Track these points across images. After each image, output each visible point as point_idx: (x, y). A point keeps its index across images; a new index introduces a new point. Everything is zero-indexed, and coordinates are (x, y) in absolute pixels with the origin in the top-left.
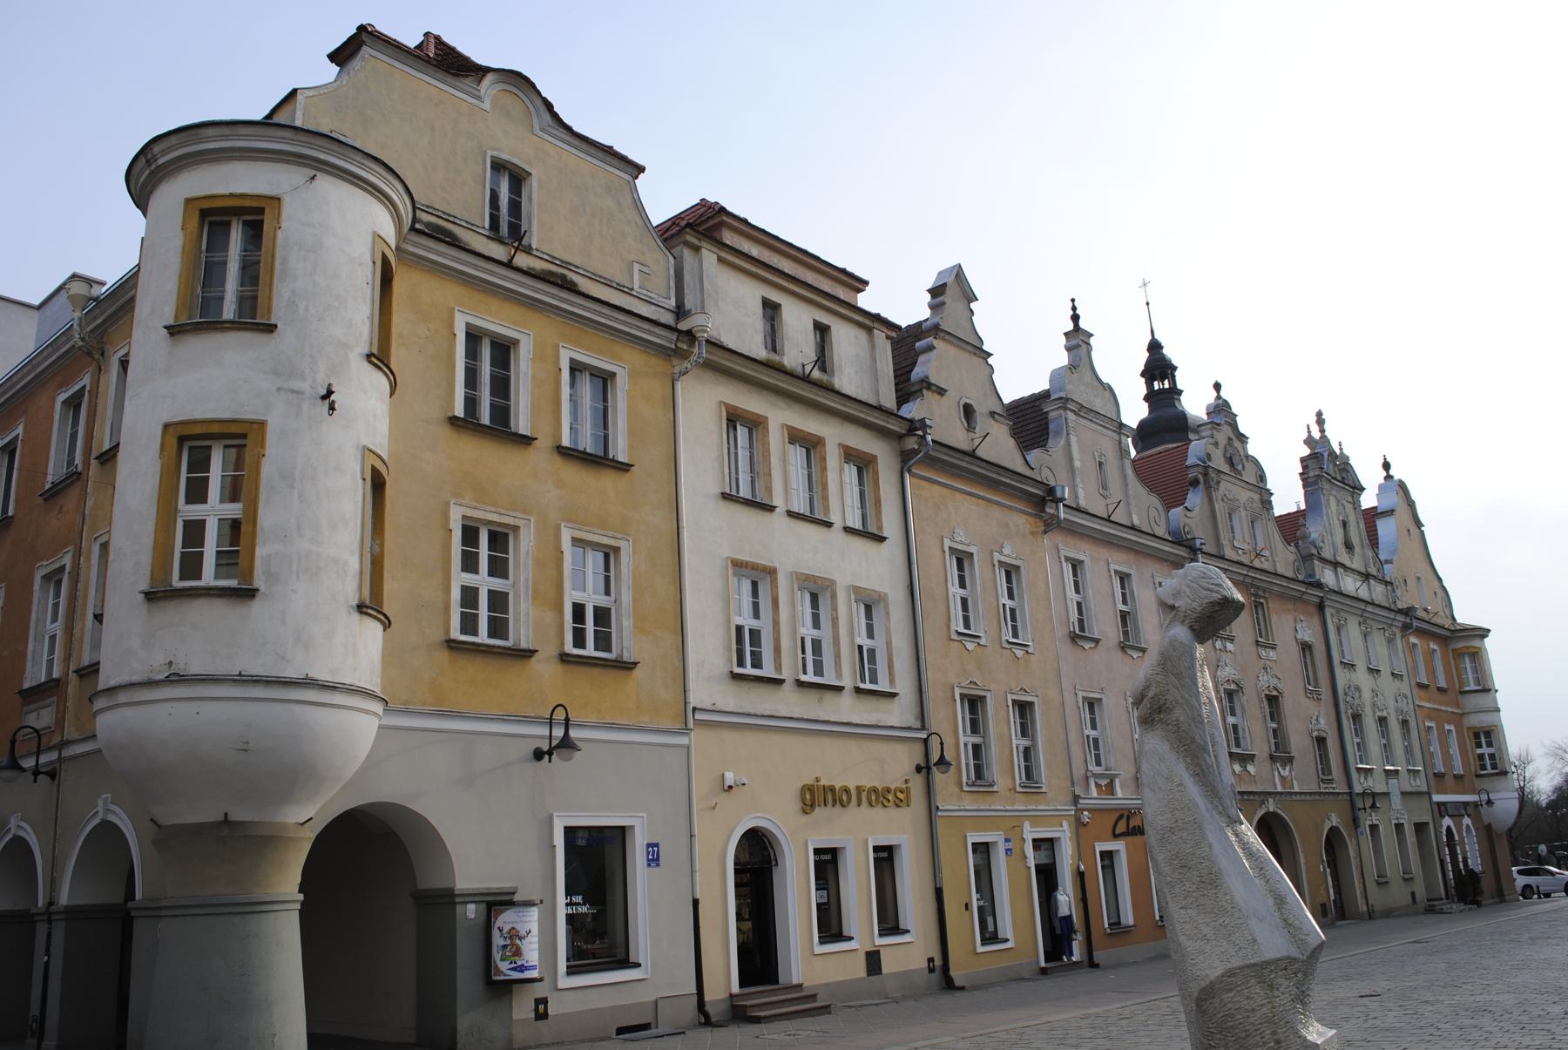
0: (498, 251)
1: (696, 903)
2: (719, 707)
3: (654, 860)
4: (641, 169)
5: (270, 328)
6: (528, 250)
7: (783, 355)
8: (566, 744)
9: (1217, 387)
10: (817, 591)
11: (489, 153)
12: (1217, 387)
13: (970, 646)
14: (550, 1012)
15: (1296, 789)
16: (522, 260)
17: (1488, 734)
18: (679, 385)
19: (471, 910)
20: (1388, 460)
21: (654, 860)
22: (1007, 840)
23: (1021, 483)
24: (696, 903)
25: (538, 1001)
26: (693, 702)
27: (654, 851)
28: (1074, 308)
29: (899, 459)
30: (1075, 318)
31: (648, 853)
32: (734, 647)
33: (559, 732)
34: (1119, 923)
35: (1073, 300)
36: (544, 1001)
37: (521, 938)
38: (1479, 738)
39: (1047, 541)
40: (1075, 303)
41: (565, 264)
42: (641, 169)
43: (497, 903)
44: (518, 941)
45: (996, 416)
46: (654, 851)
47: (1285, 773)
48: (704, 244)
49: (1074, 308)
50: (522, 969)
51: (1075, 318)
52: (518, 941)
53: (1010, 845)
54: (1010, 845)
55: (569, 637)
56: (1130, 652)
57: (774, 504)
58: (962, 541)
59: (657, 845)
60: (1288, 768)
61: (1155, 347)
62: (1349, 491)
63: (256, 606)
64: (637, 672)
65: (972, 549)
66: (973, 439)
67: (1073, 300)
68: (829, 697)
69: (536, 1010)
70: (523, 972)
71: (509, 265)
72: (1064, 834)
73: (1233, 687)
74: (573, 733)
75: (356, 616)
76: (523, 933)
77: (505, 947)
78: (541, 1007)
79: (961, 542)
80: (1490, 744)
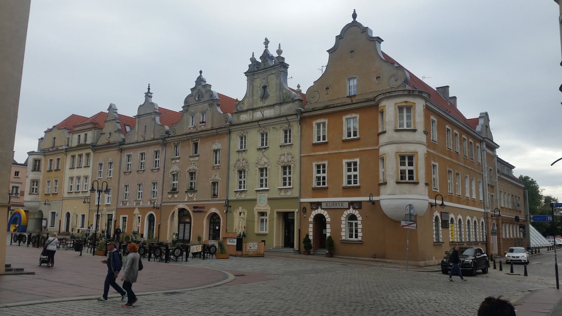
3: (57, 216)
9: (201, 72)
10: (79, 178)
12: (201, 72)
15: (195, 200)
17: (411, 158)
20: (281, 49)
21: (57, 216)
22: (101, 214)
24: (60, 221)
28: (149, 86)
30: (149, 89)
32: (79, 188)
35: (149, 84)
38: (405, 160)
47: (190, 196)
49: (149, 86)
51: (149, 89)
53: (102, 215)
54: (102, 215)
56: (153, 171)
60: (193, 195)
62: (272, 69)
65: (103, 162)
67: (149, 84)
68: (78, 193)
72: (114, 213)
73: (175, 173)
79: (101, 162)
80: (411, 164)
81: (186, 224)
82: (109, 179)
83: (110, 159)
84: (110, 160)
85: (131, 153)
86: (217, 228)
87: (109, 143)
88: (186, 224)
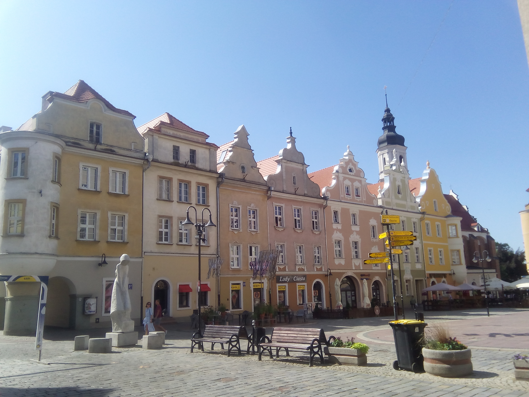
0: (92, 146)
1: (142, 298)
2: (153, 251)
4: (135, 117)
5: (27, 179)
6: (101, 144)
7: (179, 160)
8: (105, 262)
11: (90, 121)
13: (236, 232)
14: (100, 321)
16: (99, 147)
18: (144, 173)
19: (80, 299)
22: (244, 283)
23: (259, 187)
24: (142, 298)
25: (97, 319)
26: (144, 250)
27: (130, 286)
28: (291, 130)
29: (217, 184)
30: (291, 133)
31: (129, 286)
33: (103, 259)
34: (356, 307)
35: (291, 128)
36: (98, 319)
37: (91, 305)
39: (269, 202)
40: (291, 128)
41: (112, 146)
42: (135, 117)
43: (86, 298)
44: (90, 306)
45: (253, 168)
46: (130, 286)
48: (154, 134)
49: (291, 130)
50: (91, 312)
51: (291, 133)
52: (90, 306)
55: (109, 238)
57: (173, 200)
58: (236, 204)
59: (132, 284)
61: (388, 111)
63: (25, 238)
64: (128, 245)
66: (244, 175)
67: (291, 128)
69: (96, 320)
70: (91, 312)
71: (95, 150)
74: (107, 259)
75: (48, 239)
76: (92, 304)
77: (87, 307)
78: (97, 320)
81: (347, 292)
82: (253, 233)
83: (252, 205)
84: (253, 206)
85: (283, 205)
86: (374, 294)
87: (243, 180)
88: (347, 292)
